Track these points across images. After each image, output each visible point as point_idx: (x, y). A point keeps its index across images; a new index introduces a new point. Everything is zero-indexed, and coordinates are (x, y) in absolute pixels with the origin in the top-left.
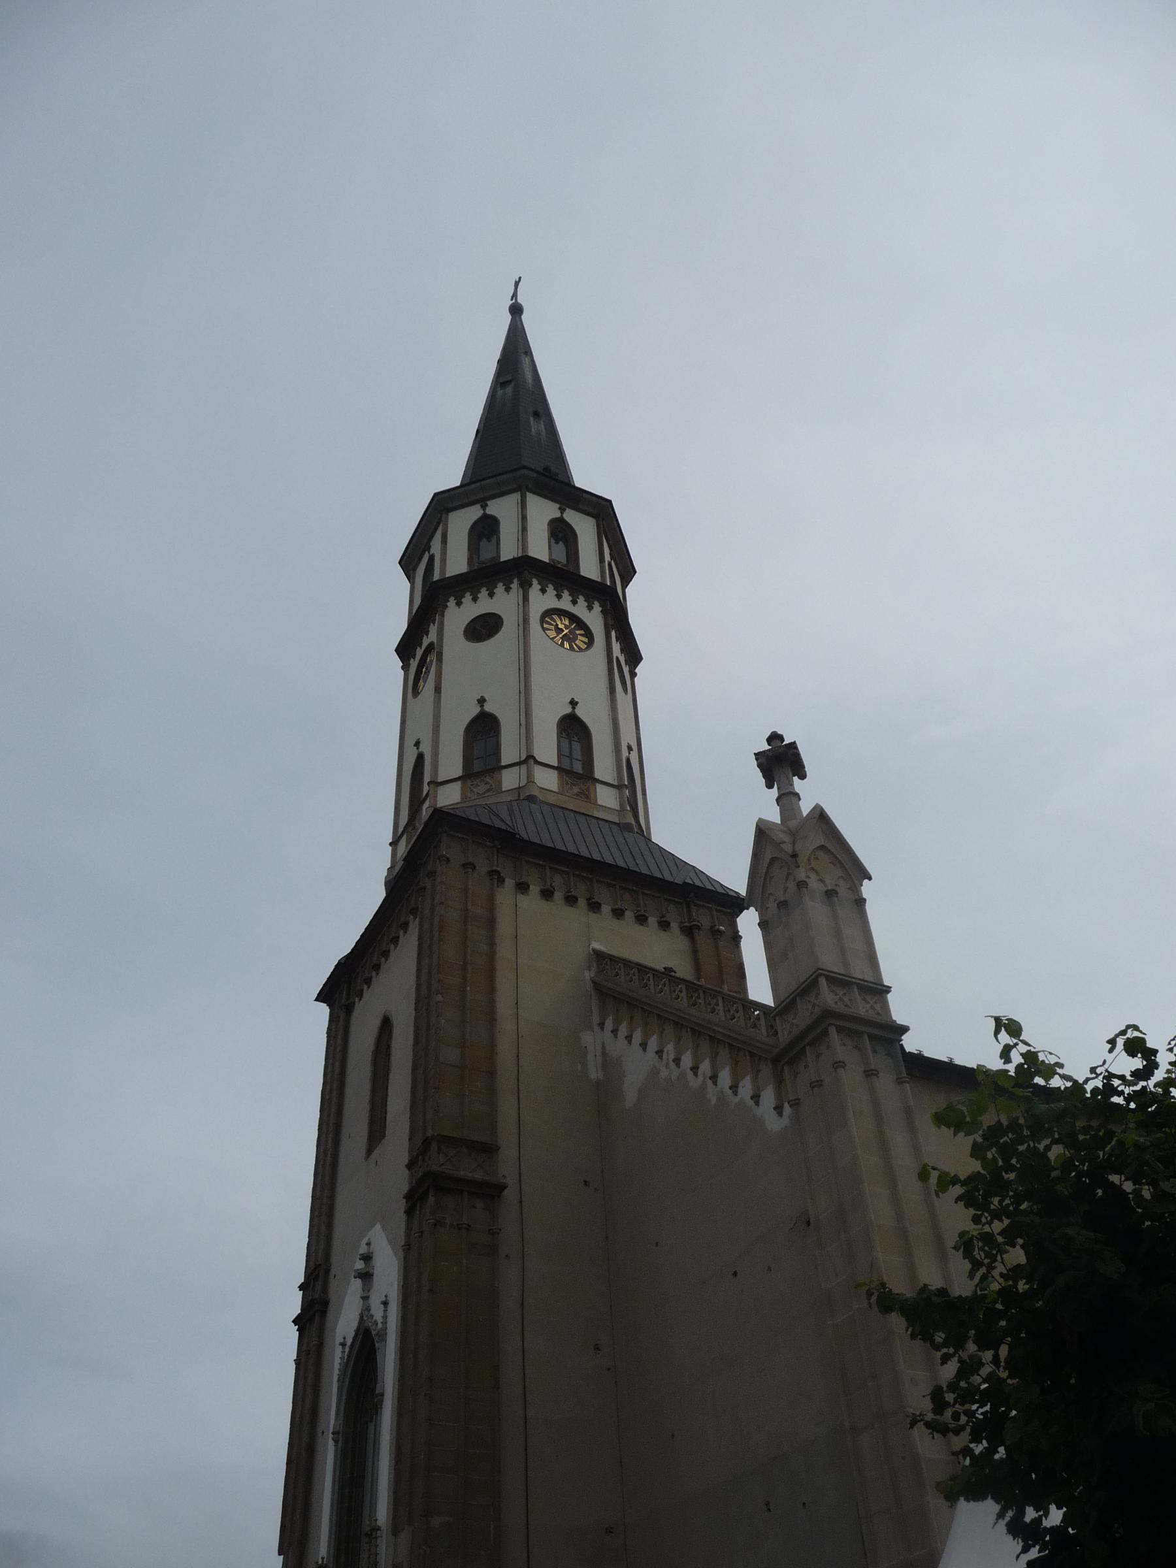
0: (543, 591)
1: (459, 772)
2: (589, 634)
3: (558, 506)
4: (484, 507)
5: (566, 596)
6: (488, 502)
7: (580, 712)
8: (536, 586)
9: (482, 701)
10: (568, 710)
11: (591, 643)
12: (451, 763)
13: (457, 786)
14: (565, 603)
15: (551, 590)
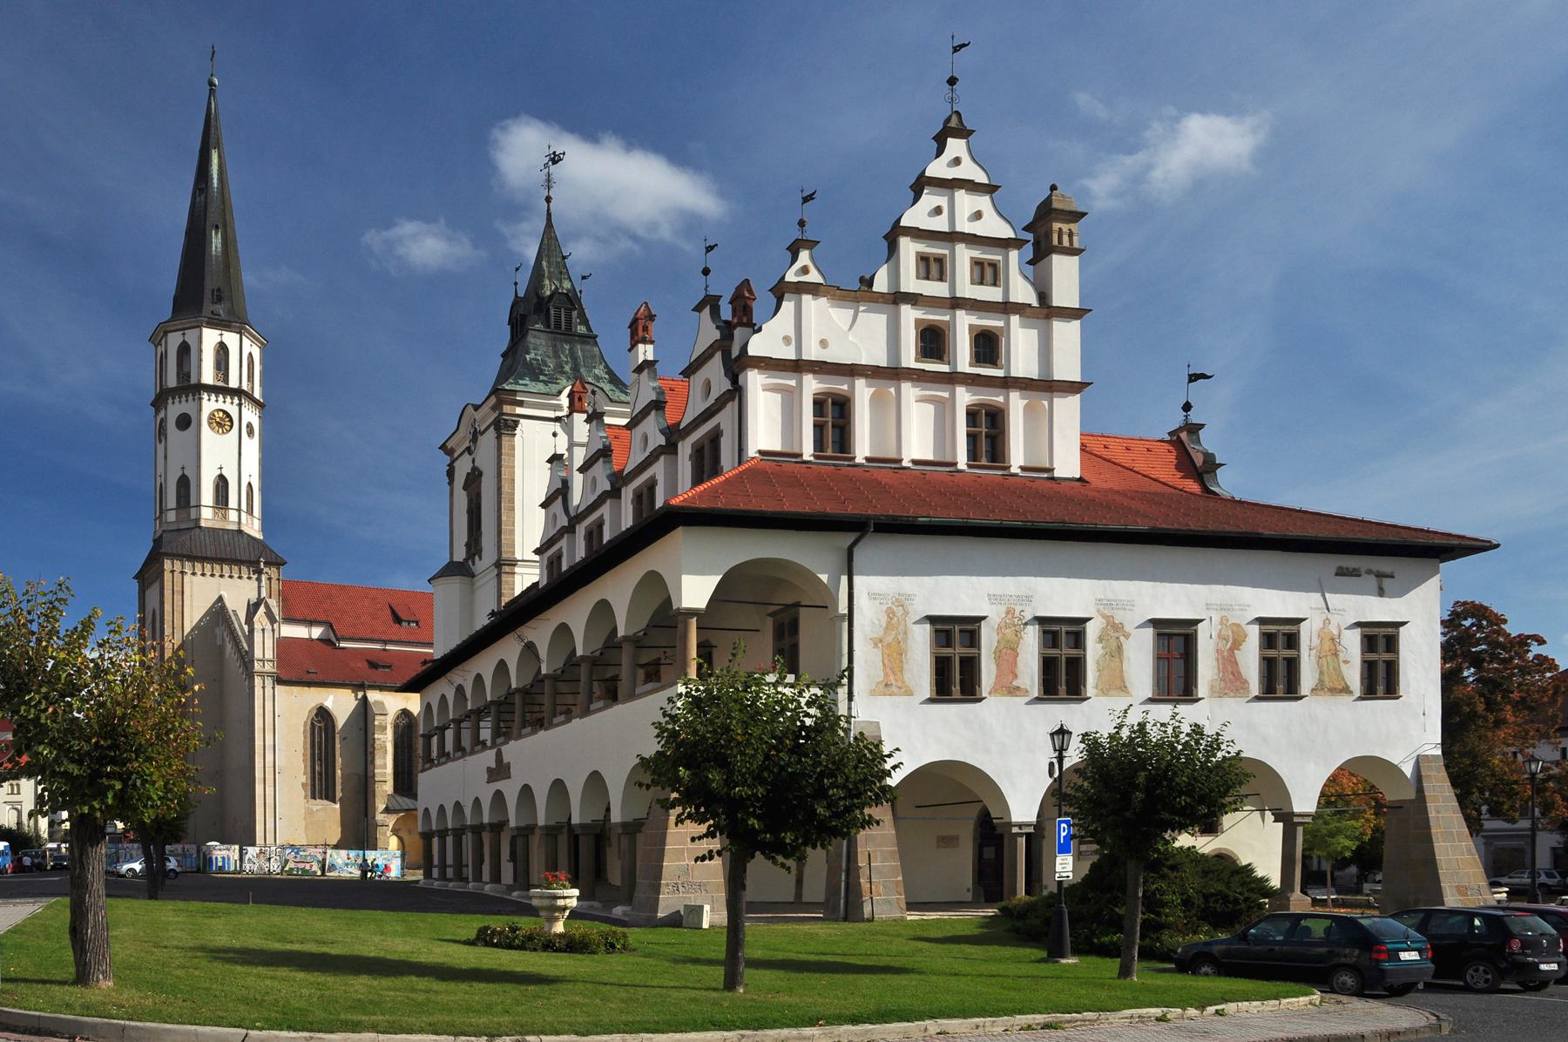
0: (209, 400)
1: (175, 507)
2: (231, 421)
3: (219, 332)
4: (184, 334)
5: (221, 398)
6: (186, 332)
7: (224, 474)
8: (205, 396)
9: (183, 468)
10: (218, 472)
11: (231, 427)
12: (171, 501)
13: (174, 512)
14: (220, 405)
15: (213, 397)
